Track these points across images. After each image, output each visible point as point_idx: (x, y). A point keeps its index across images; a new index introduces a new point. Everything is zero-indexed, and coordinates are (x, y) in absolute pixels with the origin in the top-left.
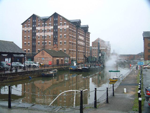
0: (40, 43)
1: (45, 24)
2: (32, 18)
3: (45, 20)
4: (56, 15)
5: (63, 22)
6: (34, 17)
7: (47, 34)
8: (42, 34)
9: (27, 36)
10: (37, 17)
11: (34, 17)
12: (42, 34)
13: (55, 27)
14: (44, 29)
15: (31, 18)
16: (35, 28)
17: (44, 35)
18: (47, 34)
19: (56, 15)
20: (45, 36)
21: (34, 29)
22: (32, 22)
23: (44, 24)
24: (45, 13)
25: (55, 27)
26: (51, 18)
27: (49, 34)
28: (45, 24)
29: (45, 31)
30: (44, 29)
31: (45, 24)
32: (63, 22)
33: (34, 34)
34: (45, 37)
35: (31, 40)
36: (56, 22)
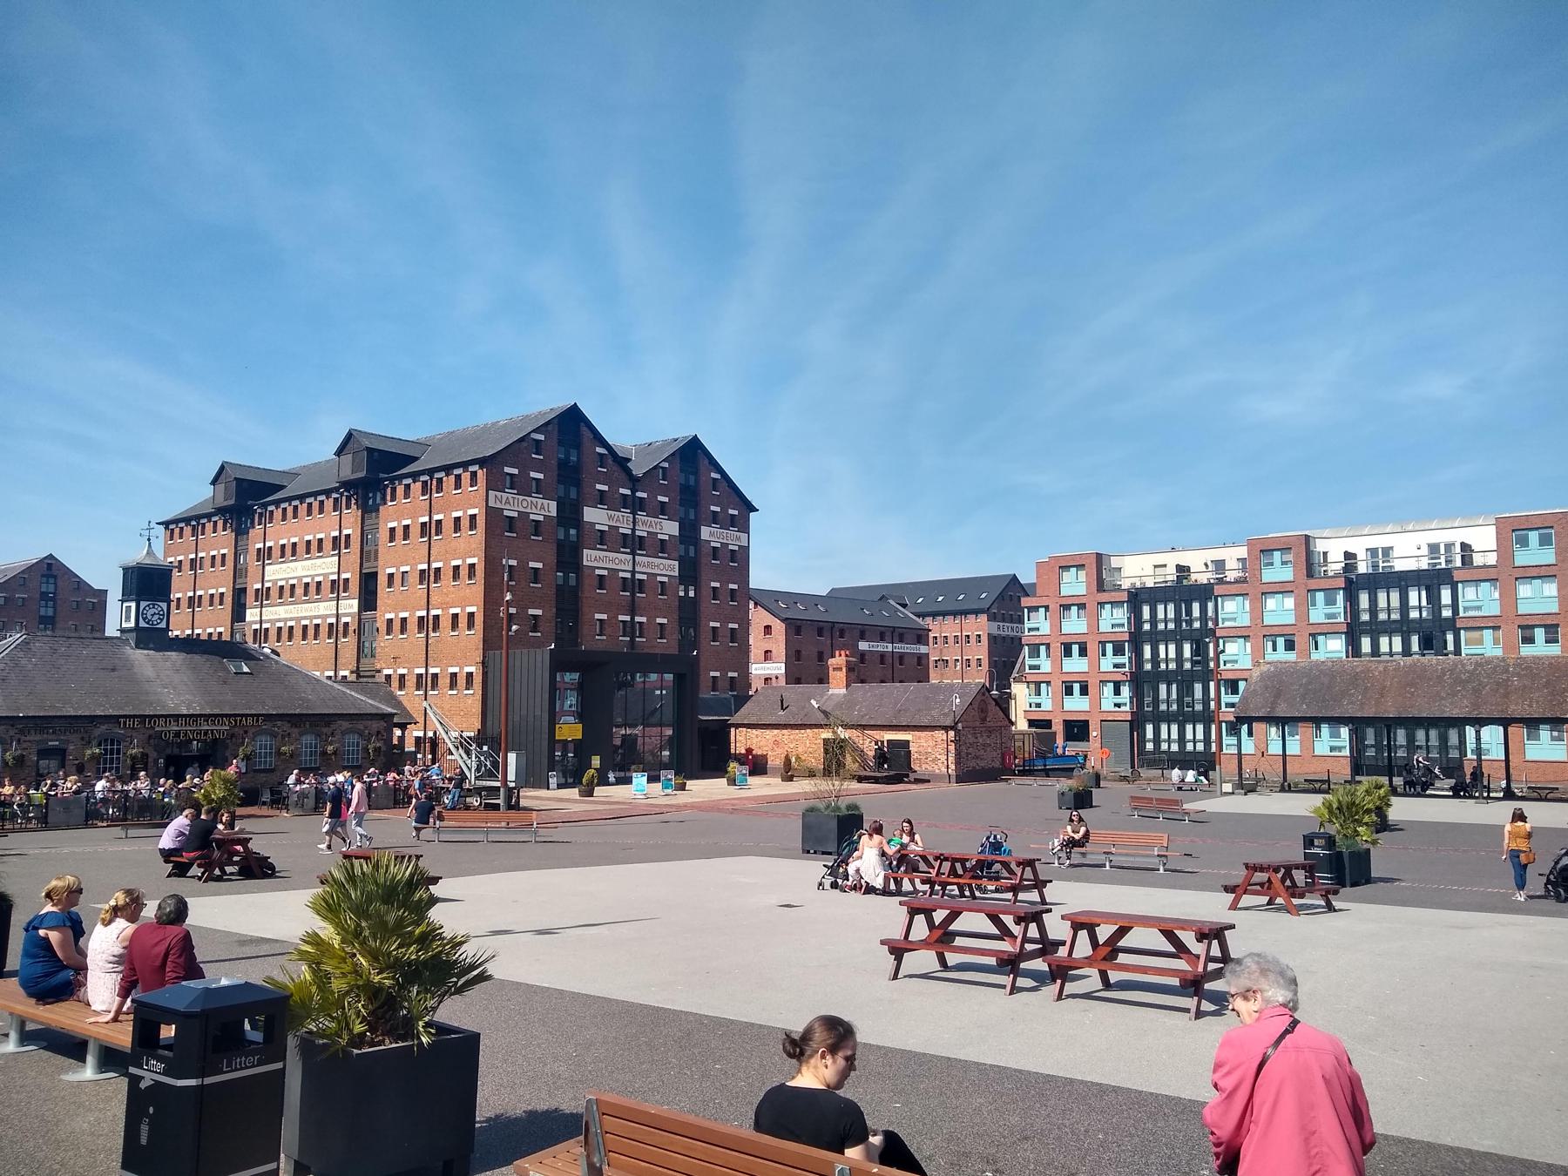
0: (608, 630)
1: (634, 491)
2: (553, 429)
4: (692, 453)
5: (724, 510)
6: (571, 425)
9: (523, 564)
11: (571, 425)
13: (689, 533)
14: (634, 530)
17: (633, 572)
19: (692, 453)
20: (638, 576)
21: (570, 514)
25: (689, 533)
30: (634, 530)
31: (634, 491)
32: (724, 510)
33: (568, 557)
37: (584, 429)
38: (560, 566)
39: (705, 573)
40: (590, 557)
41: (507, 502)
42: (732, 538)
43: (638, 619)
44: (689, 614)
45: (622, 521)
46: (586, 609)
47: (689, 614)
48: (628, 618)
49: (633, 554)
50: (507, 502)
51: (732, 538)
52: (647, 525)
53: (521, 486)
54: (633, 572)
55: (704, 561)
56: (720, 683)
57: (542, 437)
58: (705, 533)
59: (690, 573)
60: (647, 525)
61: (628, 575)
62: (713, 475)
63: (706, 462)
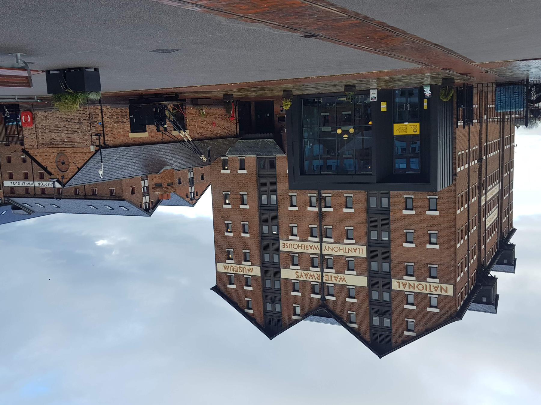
0: (342, 201)
1: (323, 298)
2: (396, 339)
3: (323, 311)
4: (272, 327)
5: (240, 288)
7: (312, 247)
8: (331, 248)
9: (421, 244)
10: (368, 338)
12: (331, 248)
13: (271, 271)
14: (322, 271)
15: (399, 340)
16: (372, 284)
17: (321, 242)
18: (312, 247)
19: (272, 327)
20: (317, 239)
21: (379, 281)
22: (395, 316)
23: (328, 298)
24: (323, 344)
26: (294, 317)
27: (300, 243)
28: (319, 296)
29: (323, 262)
30: (322, 271)
31: (323, 298)
32: (240, 288)
33: (379, 251)
34: (323, 234)
35: (394, 226)
36: (271, 295)
37: (368, 338)
38: (387, 245)
39: (256, 241)
40: (362, 252)
41: (436, 289)
42: (230, 267)
43: (316, 209)
44: (268, 214)
45: (331, 277)
46: (364, 215)
47: (268, 214)
48: (324, 209)
49: (322, 255)
50: (436, 289)
51: (230, 267)
52: (313, 275)
53: (423, 299)
54: (321, 242)
55: (257, 252)
56: (238, 164)
57: (406, 333)
58: (257, 271)
59: (269, 244)
60: (313, 275)
61: (325, 240)
62: (251, 312)
63: (258, 320)
